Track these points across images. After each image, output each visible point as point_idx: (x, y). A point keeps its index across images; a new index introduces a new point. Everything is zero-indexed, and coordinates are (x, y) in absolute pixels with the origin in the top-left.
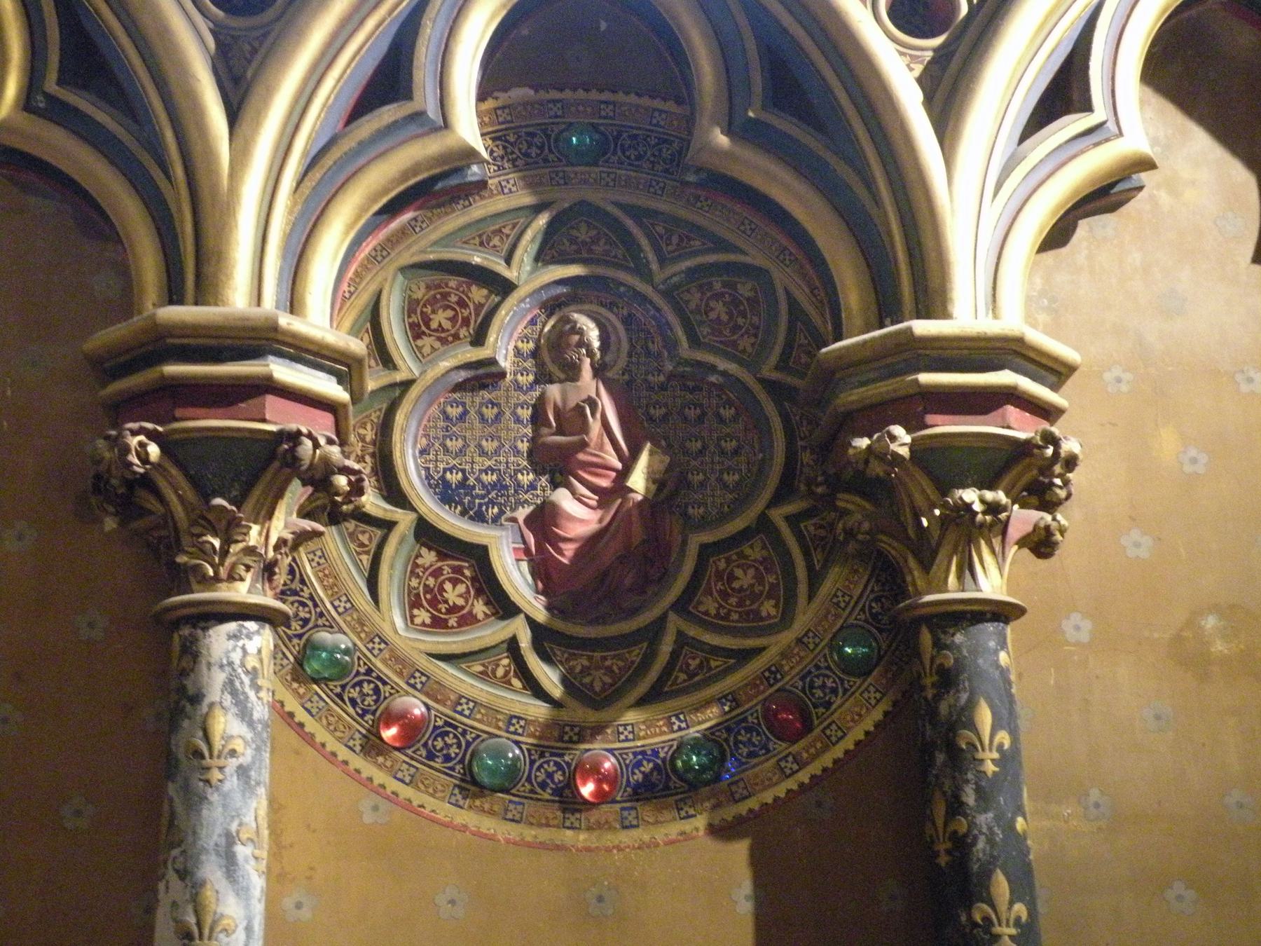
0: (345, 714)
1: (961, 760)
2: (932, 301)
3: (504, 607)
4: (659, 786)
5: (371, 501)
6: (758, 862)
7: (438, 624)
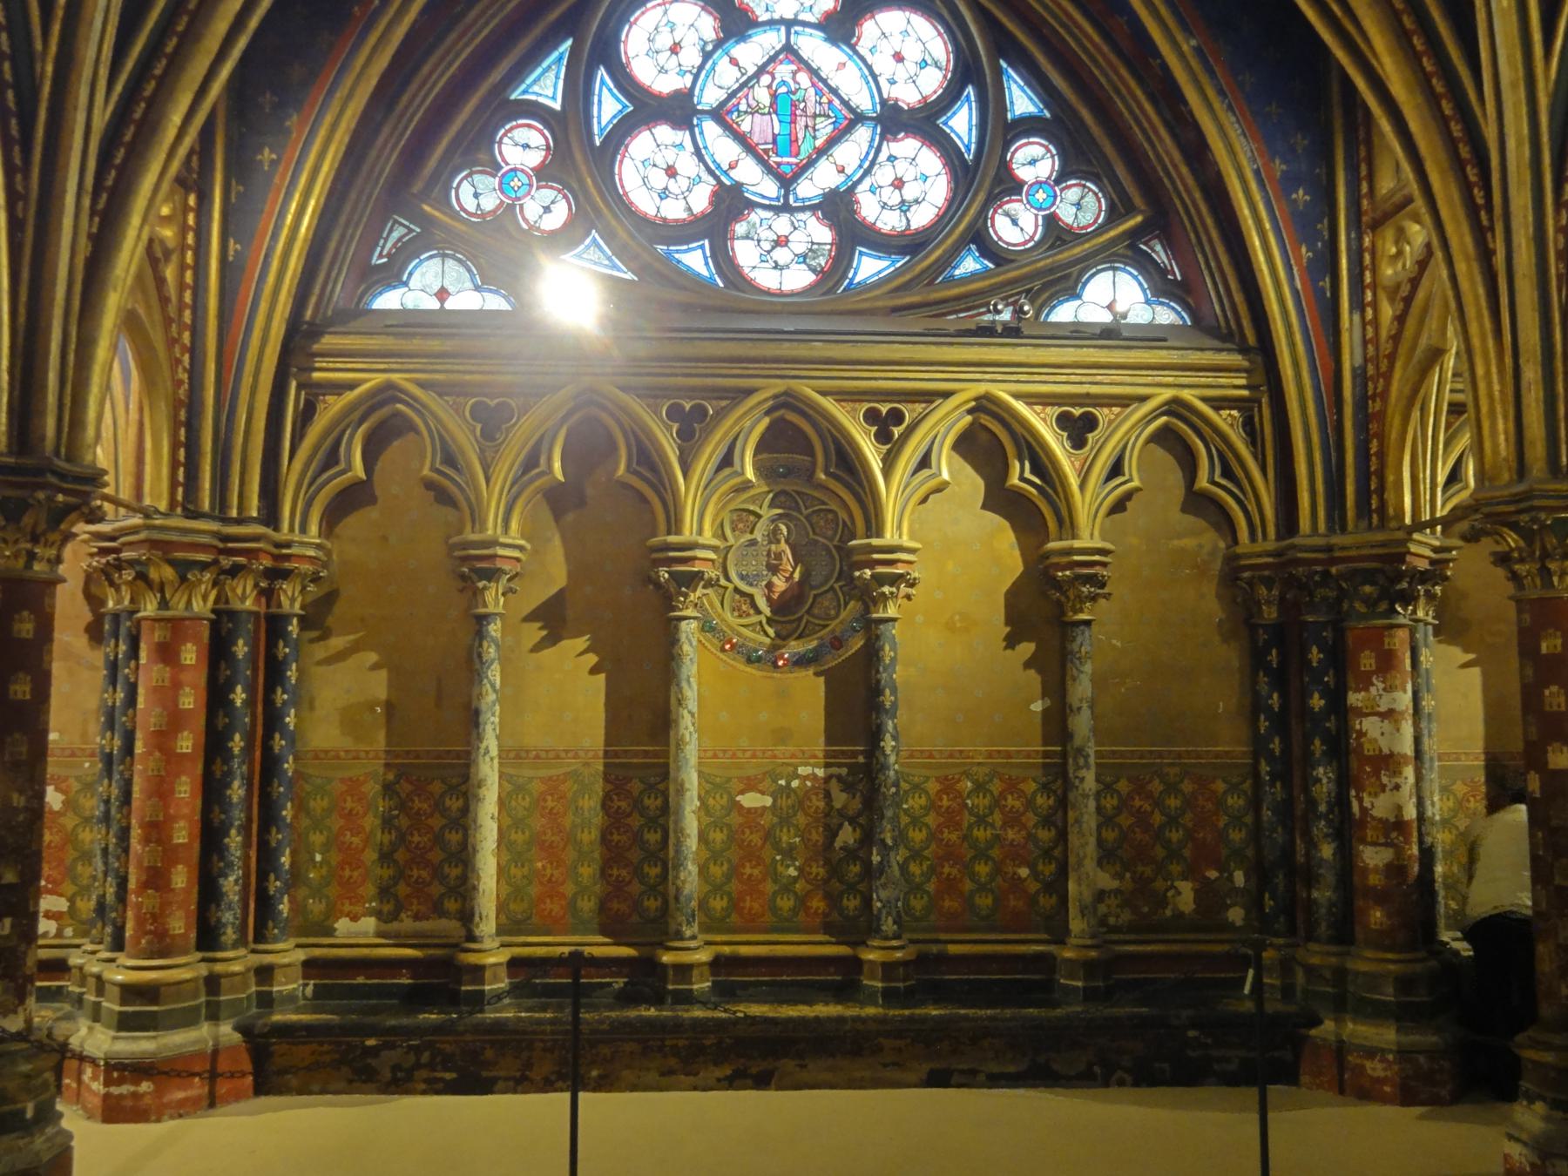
0: (715, 641)
1: (879, 659)
3: (758, 612)
4: (801, 662)
5: (723, 582)
6: (827, 683)
7: (740, 616)
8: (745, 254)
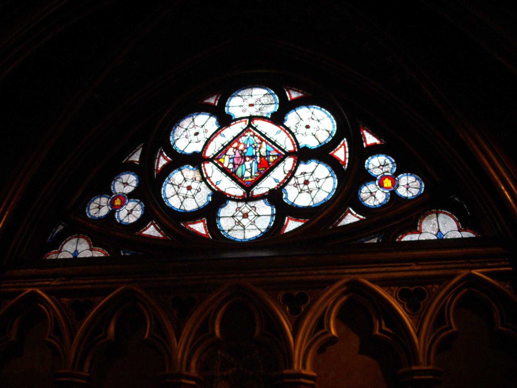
2: (291, 366)
8: (225, 223)
